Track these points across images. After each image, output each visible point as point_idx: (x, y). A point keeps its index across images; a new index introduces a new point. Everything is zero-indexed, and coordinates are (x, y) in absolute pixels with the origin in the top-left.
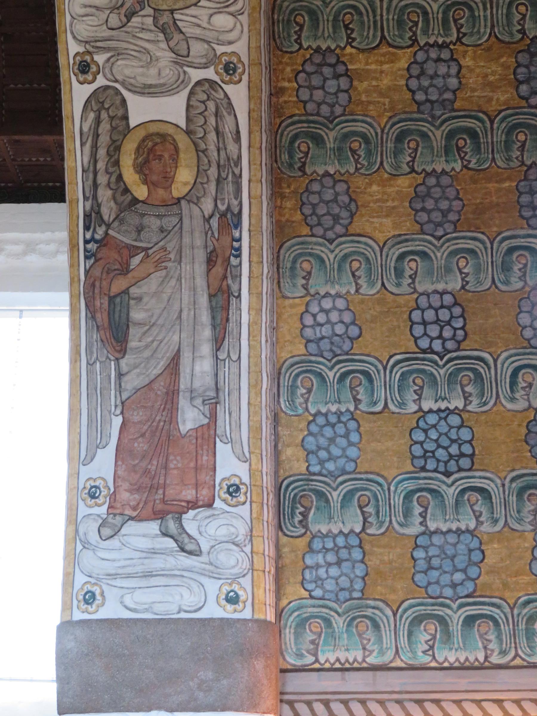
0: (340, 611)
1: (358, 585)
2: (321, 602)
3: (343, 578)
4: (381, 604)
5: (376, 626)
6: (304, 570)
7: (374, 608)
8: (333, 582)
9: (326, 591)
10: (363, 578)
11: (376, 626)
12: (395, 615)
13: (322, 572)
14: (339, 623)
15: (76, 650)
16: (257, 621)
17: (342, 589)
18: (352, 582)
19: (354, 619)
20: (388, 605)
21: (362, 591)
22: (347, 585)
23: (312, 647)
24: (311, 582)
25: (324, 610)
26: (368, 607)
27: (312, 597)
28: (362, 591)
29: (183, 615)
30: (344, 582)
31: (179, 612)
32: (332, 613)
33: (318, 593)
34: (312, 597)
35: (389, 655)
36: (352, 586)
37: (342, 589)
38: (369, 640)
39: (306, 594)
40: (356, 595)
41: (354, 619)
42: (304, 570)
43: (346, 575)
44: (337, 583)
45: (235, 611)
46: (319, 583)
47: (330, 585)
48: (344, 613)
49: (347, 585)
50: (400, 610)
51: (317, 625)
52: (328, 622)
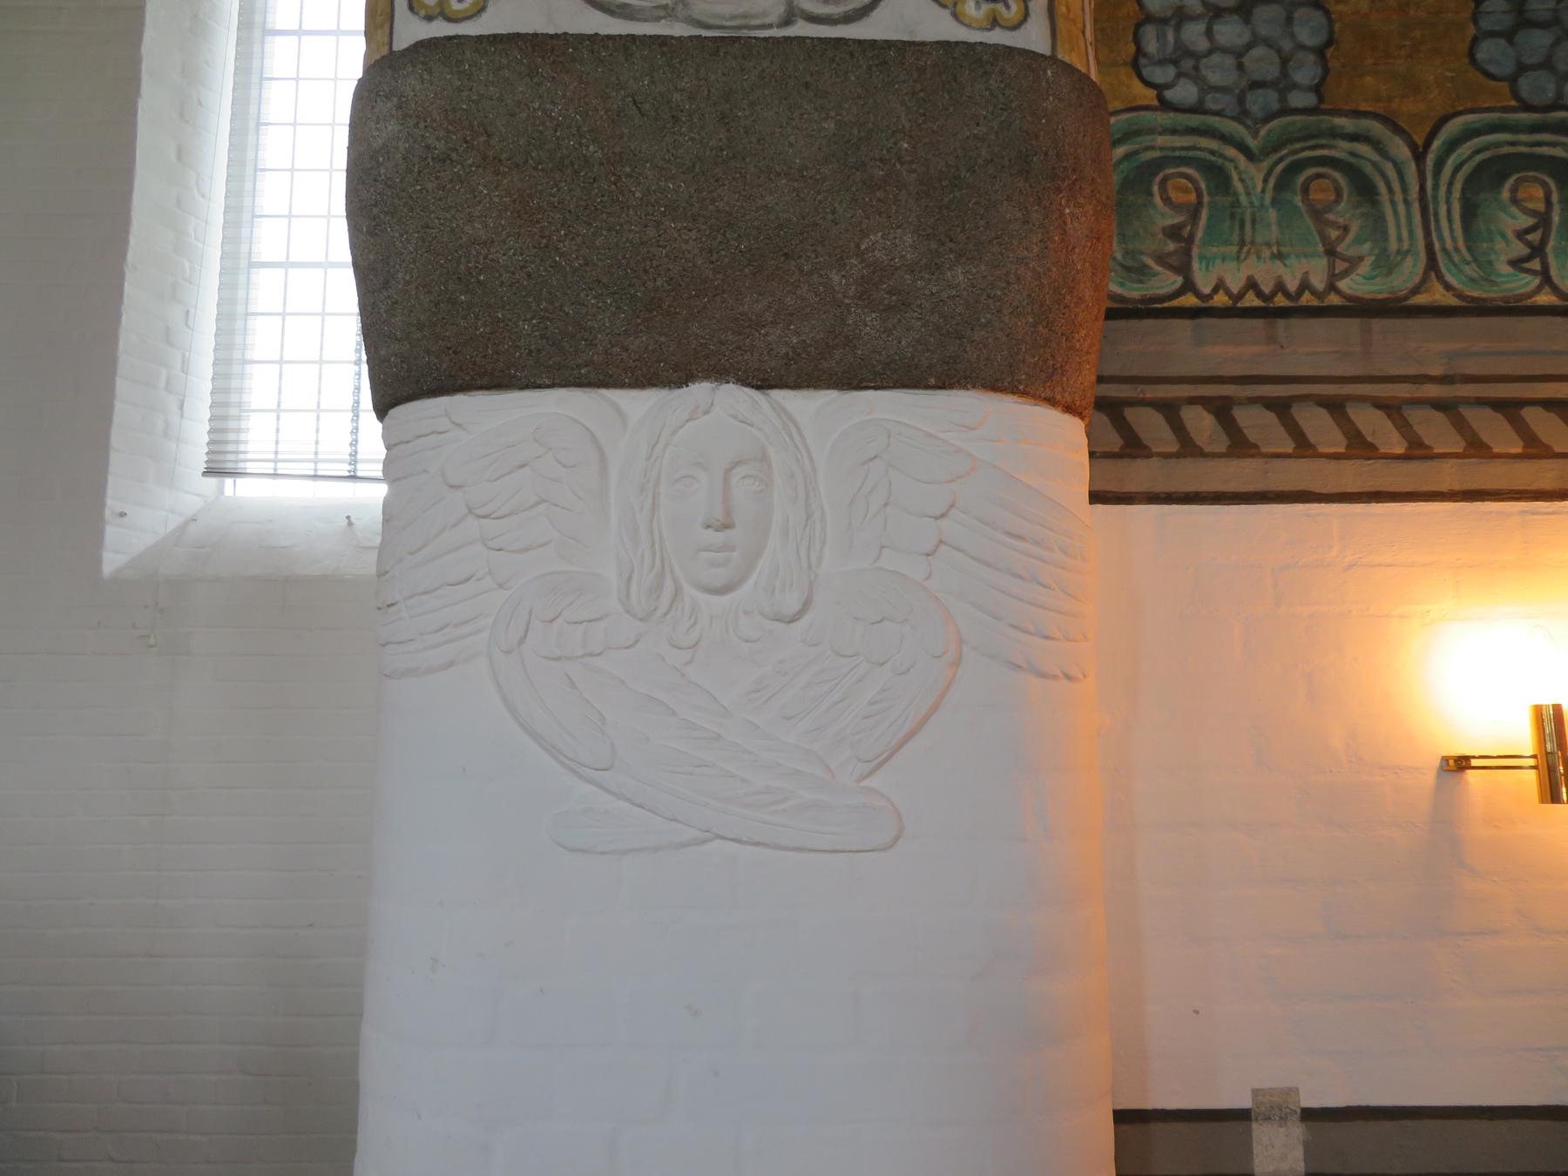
0: (1253, 144)
1: (1306, 72)
2: (1195, 120)
3: (1259, 52)
4: (1376, 128)
5: (1365, 190)
6: (1138, 26)
7: (1354, 138)
8: (1229, 61)
9: (1207, 89)
10: (1320, 52)
11: (1365, 190)
12: (1419, 156)
13: (1194, 34)
14: (1251, 179)
15: (402, 146)
16: (1068, 69)
17: (1256, 85)
18: (1285, 62)
19: (1295, 168)
20: (1397, 129)
21: (1317, 89)
22: (1271, 71)
23: (1171, 246)
24: (1161, 63)
25: (1204, 142)
26: (1335, 134)
27: (1165, 105)
28: (1317, 89)
29: (801, 29)
30: (1262, 63)
31: (787, 22)
32: (1231, 152)
33: (1184, 92)
34: (1165, 105)
35: (1410, 271)
36: (1284, 74)
37: (1256, 85)
38: (1346, 229)
39: (1149, 96)
40: (1299, 99)
41: (1295, 168)
42: (1138, 26)
43: (1268, 43)
44: (1240, 67)
45: (994, 22)
46: (1187, 64)
47: (1219, 72)
48: (1266, 152)
49: (1271, 71)
50: (1436, 144)
51: (1184, 185)
52: (1218, 176)
